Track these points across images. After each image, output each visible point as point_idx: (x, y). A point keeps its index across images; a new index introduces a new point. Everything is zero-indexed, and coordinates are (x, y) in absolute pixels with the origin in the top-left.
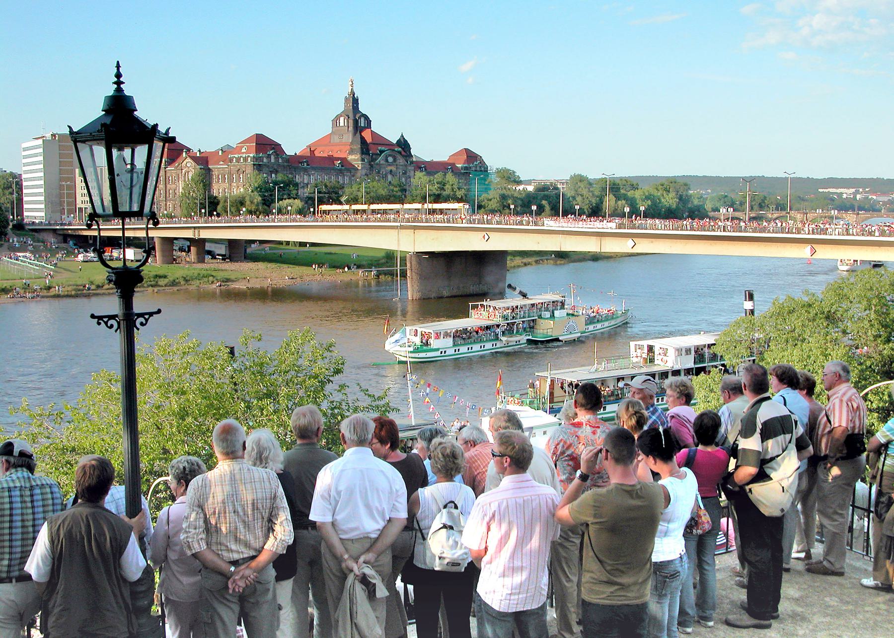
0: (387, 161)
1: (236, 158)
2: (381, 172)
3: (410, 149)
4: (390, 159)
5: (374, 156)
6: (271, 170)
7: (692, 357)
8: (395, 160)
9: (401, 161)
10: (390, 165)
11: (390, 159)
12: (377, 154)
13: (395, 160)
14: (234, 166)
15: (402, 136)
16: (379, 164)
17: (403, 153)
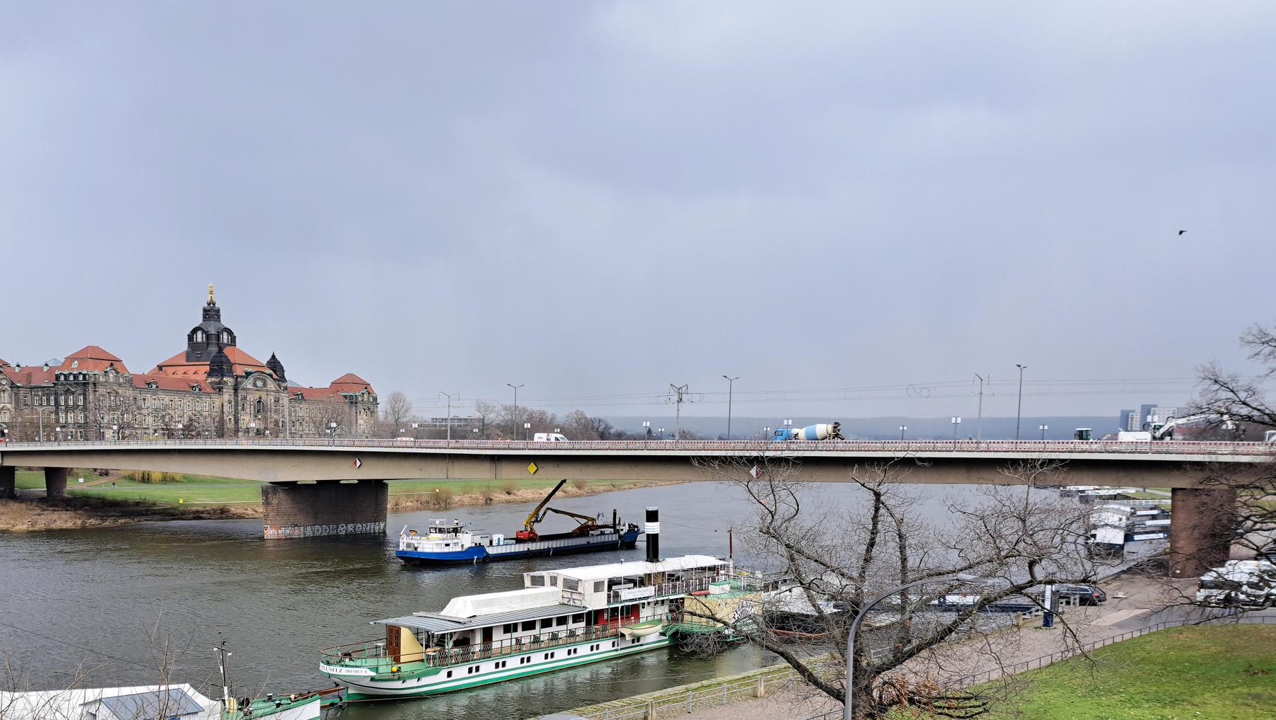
0: (255, 385)
1: (64, 375)
2: (248, 399)
3: (284, 371)
4: (259, 383)
5: (239, 379)
6: (109, 391)
7: (604, 594)
9: (271, 385)
10: (258, 390)
11: (259, 383)
12: (241, 377)
13: (265, 384)
14: (62, 384)
15: (273, 356)
17: (275, 376)
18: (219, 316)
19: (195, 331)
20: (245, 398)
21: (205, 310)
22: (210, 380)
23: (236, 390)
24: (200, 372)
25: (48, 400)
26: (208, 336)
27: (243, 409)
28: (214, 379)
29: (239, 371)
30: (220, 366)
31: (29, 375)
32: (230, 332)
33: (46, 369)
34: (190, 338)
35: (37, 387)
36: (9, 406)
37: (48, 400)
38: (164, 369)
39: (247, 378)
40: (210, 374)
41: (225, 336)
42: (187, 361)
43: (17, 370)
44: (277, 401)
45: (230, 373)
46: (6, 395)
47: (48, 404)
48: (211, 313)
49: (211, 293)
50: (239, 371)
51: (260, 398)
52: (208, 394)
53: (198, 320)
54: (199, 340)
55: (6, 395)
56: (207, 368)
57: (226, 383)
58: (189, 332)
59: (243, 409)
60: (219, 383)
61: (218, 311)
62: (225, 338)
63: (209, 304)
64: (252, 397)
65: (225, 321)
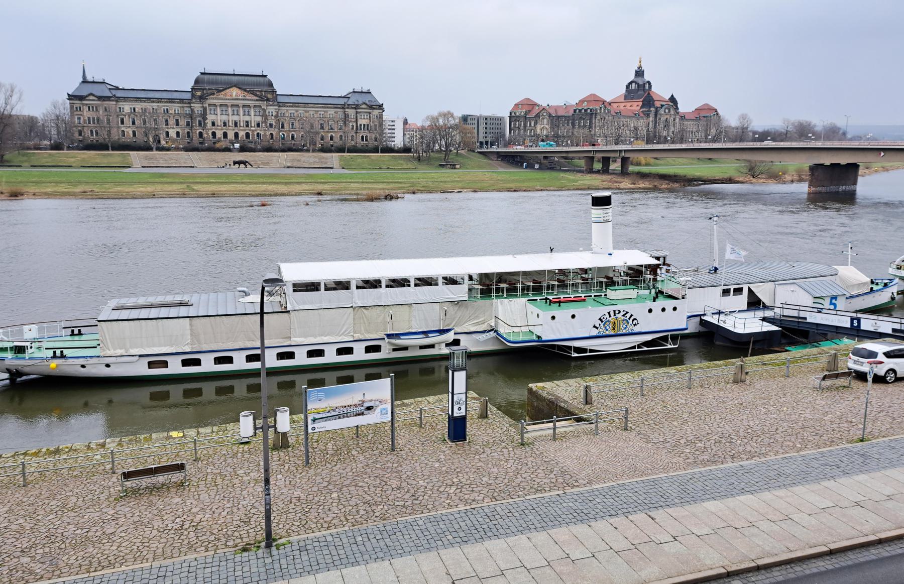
0: (665, 112)
8: (669, 112)
9: (672, 112)
11: (667, 111)
13: (669, 112)
15: (672, 96)
16: (661, 114)
18: (643, 74)
19: (631, 83)
20: (660, 119)
21: (636, 71)
22: (642, 110)
23: (656, 115)
24: (636, 106)
25: (568, 123)
26: (639, 85)
27: (659, 125)
28: (644, 109)
29: (658, 104)
30: (649, 101)
31: (556, 111)
32: (649, 83)
33: (564, 107)
34: (627, 87)
35: (562, 116)
36: (547, 126)
37: (568, 123)
38: (612, 104)
39: (661, 108)
40: (642, 107)
41: (647, 85)
42: (625, 99)
43: (548, 107)
44: (674, 120)
45: (654, 105)
46: (545, 120)
47: (568, 125)
48: (639, 73)
49: (640, 62)
50: (658, 104)
51: (667, 119)
52: (642, 117)
53: (632, 77)
54: (633, 88)
55: (545, 120)
56: (641, 104)
57: (651, 111)
58: (626, 83)
59: (659, 125)
60: (648, 111)
61: (643, 71)
62: (647, 85)
63: (639, 68)
64: (663, 119)
65: (647, 77)
